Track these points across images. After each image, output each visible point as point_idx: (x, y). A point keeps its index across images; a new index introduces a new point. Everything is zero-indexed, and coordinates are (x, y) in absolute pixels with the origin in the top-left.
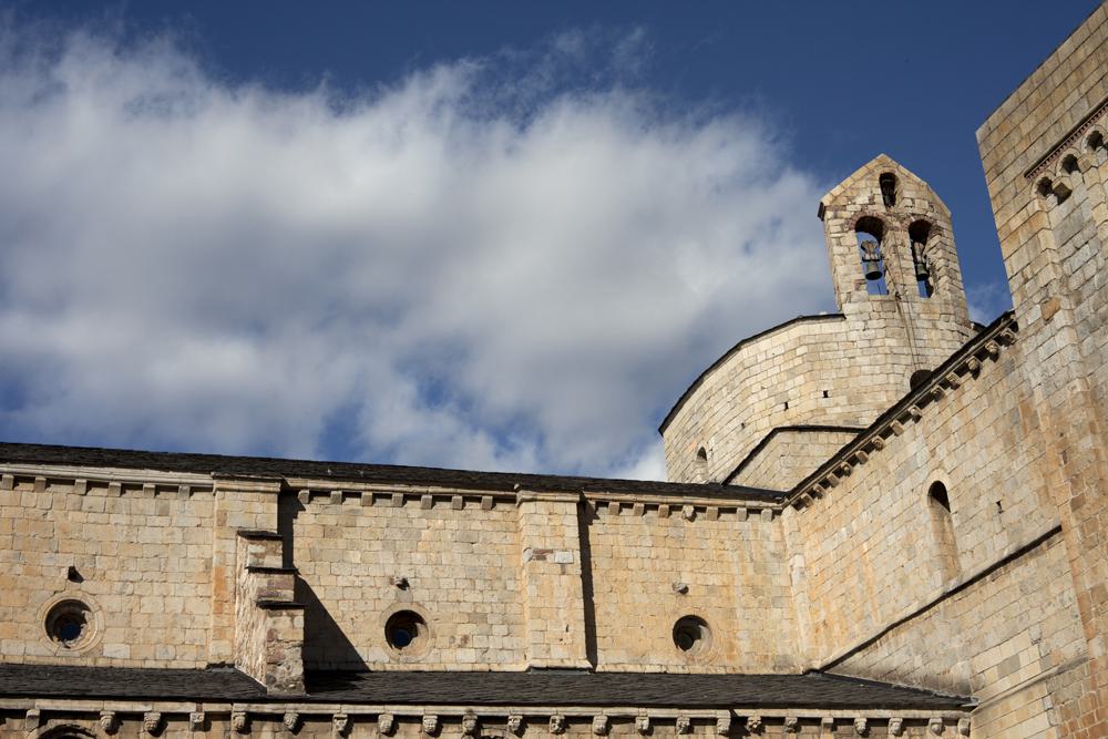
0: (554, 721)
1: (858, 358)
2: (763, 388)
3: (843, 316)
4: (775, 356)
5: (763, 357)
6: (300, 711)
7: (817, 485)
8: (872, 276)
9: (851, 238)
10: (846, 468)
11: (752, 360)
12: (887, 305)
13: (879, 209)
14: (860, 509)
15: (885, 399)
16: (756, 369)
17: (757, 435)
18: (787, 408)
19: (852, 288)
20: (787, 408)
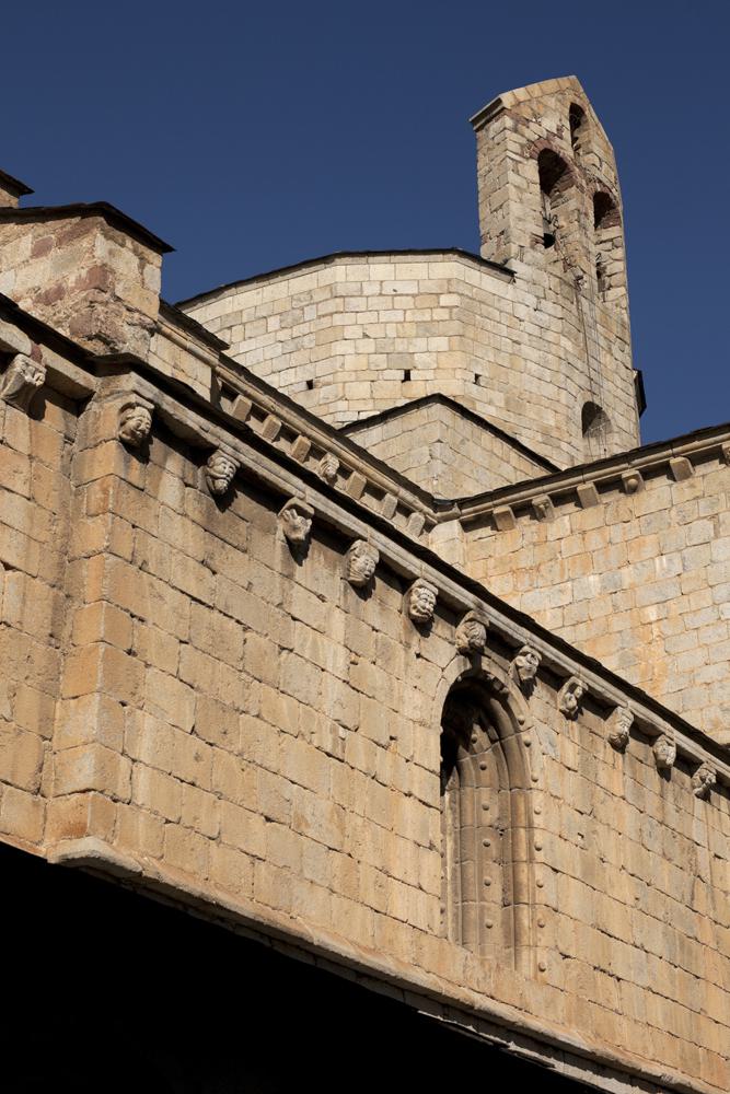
0: (573, 688)
1: (522, 346)
2: (366, 336)
3: (511, 273)
4: (396, 294)
5: (376, 289)
6: (244, 459)
7: (545, 497)
8: (549, 240)
9: (531, 170)
10: (633, 481)
11: (353, 288)
12: (567, 289)
13: (564, 148)
14: (650, 550)
15: (552, 423)
16: (354, 303)
17: (342, 405)
18: (407, 377)
19: (526, 242)
20: (407, 377)
